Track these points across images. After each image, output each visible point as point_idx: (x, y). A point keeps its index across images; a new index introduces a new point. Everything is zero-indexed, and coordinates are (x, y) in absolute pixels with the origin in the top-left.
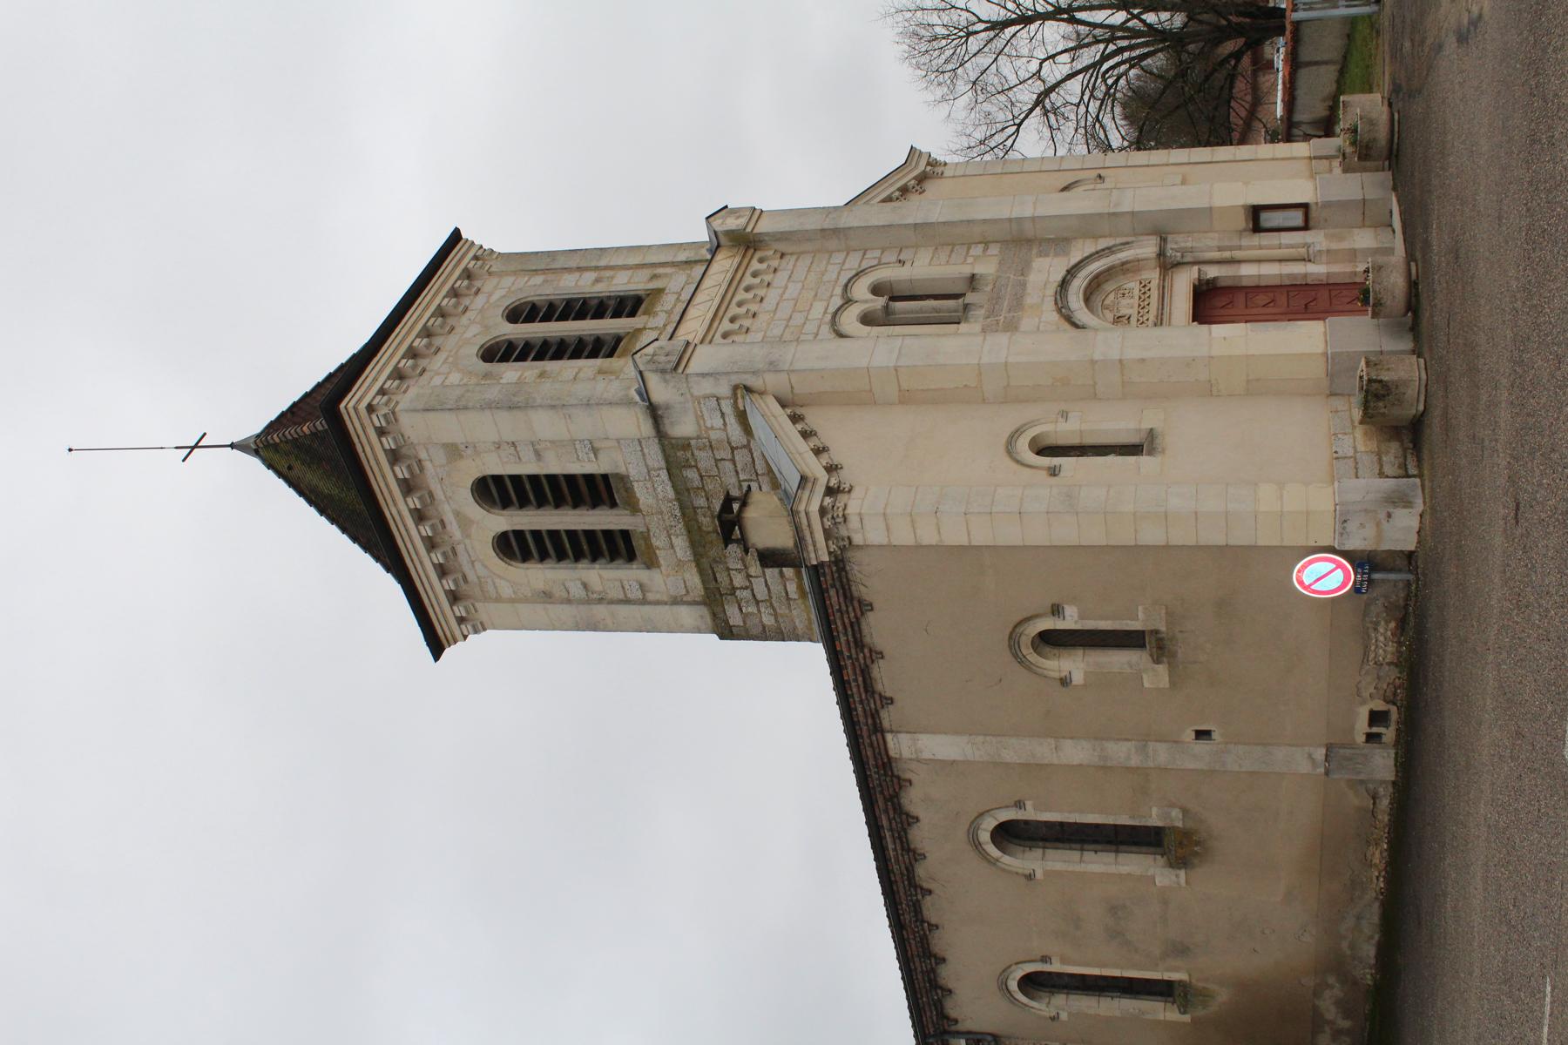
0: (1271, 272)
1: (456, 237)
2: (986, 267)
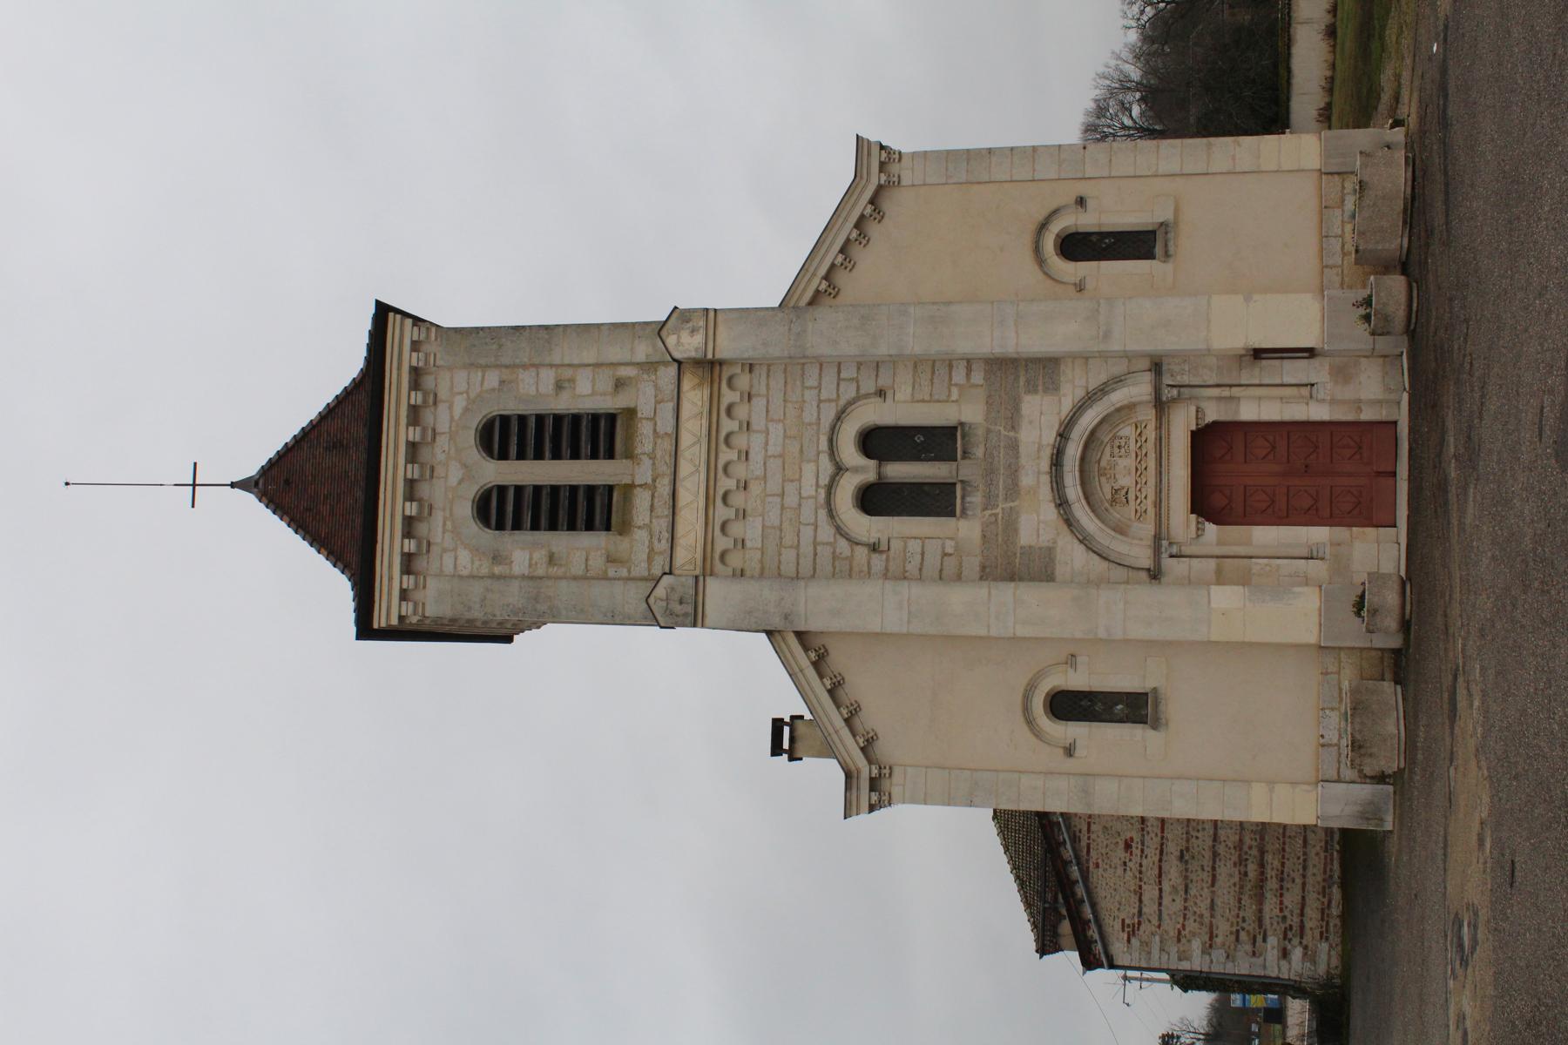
0: (1271, 411)
1: (383, 311)
2: (968, 411)
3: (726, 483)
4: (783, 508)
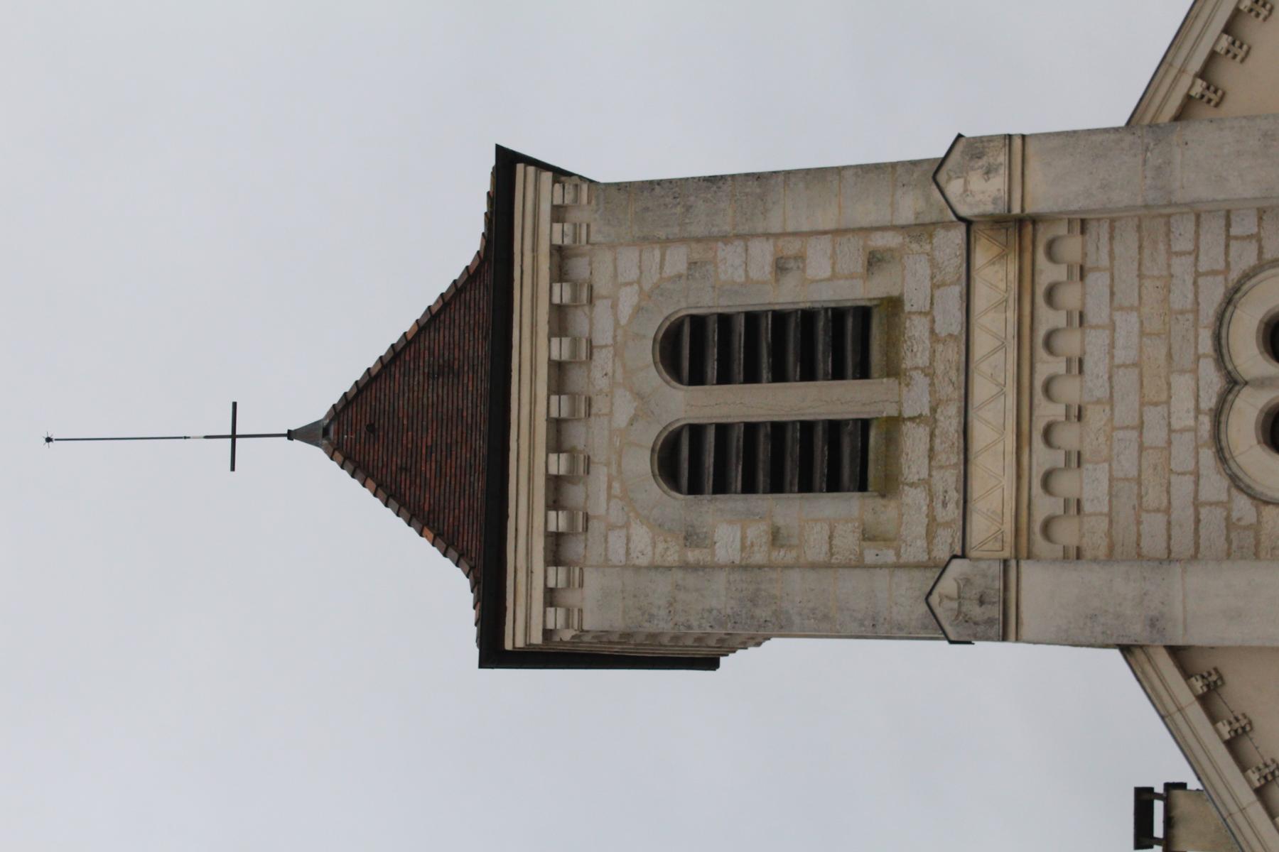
1: (507, 162)
3: (1047, 411)
4: (1141, 448)
